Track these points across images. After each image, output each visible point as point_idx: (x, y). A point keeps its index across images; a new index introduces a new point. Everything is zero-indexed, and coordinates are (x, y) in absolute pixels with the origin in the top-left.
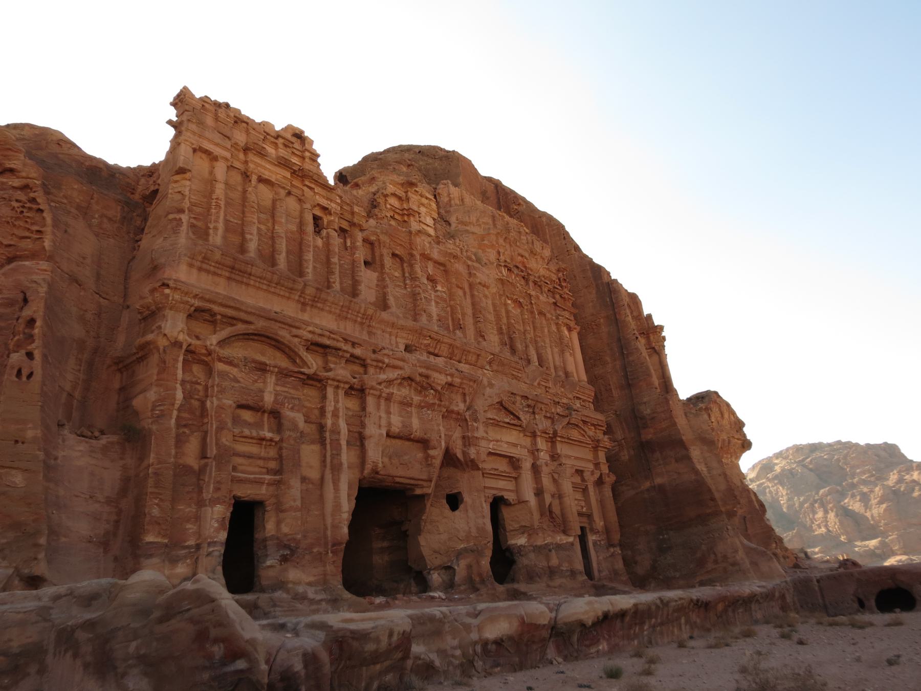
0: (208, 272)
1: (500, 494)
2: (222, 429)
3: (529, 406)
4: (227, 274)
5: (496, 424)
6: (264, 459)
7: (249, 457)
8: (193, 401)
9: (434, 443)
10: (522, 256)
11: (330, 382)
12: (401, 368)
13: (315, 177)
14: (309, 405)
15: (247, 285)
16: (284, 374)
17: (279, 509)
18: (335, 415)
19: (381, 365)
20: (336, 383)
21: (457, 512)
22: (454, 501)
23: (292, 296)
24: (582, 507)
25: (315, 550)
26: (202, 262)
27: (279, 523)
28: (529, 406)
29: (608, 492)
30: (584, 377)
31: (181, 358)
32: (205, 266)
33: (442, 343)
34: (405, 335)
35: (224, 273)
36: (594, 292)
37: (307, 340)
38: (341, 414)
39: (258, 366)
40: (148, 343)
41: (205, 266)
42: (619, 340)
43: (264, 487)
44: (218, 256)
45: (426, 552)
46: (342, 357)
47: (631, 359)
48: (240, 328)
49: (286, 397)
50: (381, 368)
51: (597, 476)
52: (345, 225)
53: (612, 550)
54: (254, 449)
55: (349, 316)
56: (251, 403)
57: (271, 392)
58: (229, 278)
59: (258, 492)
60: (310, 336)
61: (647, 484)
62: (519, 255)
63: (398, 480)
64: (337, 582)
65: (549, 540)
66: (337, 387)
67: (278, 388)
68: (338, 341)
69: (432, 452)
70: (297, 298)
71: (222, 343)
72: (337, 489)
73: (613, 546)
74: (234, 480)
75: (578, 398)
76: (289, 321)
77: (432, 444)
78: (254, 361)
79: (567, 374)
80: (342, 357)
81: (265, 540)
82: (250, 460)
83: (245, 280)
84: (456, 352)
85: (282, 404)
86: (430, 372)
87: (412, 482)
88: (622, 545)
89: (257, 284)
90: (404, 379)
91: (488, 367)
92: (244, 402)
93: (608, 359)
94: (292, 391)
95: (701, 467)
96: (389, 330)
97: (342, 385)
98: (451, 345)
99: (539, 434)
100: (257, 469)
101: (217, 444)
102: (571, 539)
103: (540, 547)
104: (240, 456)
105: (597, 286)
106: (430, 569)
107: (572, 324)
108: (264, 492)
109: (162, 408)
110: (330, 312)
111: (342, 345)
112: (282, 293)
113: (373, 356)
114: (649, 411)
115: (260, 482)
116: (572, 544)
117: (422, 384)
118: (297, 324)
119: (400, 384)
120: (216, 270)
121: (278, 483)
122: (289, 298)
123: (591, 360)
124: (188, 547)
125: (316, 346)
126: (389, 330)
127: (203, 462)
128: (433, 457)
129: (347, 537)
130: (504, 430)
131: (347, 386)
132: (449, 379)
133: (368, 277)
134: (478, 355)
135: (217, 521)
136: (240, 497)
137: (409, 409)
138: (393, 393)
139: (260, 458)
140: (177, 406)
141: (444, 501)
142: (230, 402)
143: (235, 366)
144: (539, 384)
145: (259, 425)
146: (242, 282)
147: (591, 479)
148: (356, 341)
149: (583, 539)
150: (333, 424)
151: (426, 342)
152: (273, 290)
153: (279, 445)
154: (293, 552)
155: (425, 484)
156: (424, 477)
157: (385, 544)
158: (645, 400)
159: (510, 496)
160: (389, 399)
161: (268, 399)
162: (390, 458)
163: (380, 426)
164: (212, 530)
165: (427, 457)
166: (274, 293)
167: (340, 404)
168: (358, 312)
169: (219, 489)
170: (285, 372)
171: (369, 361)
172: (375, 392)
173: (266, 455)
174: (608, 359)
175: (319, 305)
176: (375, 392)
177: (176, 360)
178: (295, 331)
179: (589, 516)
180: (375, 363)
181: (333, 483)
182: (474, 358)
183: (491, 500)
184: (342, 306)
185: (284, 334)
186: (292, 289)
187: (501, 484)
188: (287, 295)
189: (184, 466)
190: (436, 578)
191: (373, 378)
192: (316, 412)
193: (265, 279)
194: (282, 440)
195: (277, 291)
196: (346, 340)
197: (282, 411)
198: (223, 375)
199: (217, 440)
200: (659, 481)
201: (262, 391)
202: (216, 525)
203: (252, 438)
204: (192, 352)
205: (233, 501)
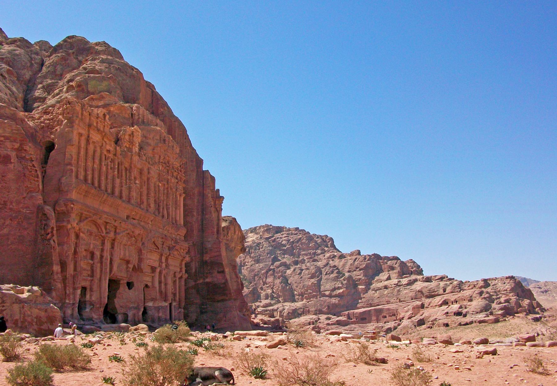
17: (91, 290)
18: (107, 252)
21: (131, 290)
22: (130, 285)
27: (91, 296)
29: (183, 283)
30: (182, 223)
36: (195, 174)
40: (63, 226)
42: (203, 205)
45: (117, 306)
47: (207, 216)
51: (180, 275)
61: (201, 281)
65: (160, 304)
69: (129, 265)
72: (105, 283)
73: (180, 308)
79: (176, 221)
81: (86, 301)
88: (185, 308)
93: (195, 214)
95: (228, 277)
105: (197, 171)
114: (210, 246)
121: (92, 280)
123: (187, 213)
133: (118, 181)
141: (126, 285)
147: (178, 276)
149: (171, 304)
158: (209, 240)
159: (150, 284)
165: (127, 267)
174: (195, 214)
190: (120, 317)
194: (94, 264)
200: (207, 280)
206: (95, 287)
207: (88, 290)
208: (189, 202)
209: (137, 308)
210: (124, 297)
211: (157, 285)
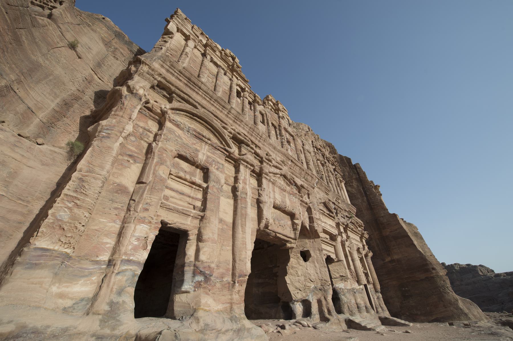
2: (162, 164)
4: (186, 82)
6: (193, 198)
7: (181, 193)
8: (142, 142)
9: (297, 216)
12: (281, 169)
14: (228, 173)
17: (200, 238)
19: (270, 163)
21: (308, 263)
23: (224, 111)
25: (225, 280)
26: (170, 67)
31: (139, 107)
34: (280, 156)
35: (183, 80)
39: (197, 135)
43: (190, 218)
45: (291, 288)
48: (188, 107)
49: (214, 161)
54: (187, 190)
55: (253, 135)
56: (188, 156)
57: (204, 154)
59: (183, 222)
61: (388, 259)
63: (278, 235)
64: (240, 309)
67: (209, 154)
70: (226, 113)
78: (195, 131)
82: (181, 196)
83: (196, 90)
85: (211, 164)
89: (204, 96)
92: (184, 154)
100: (186, 204)
101: (154, 173)
104: (174, 191)
105: (349, 166)
106: (295, 301)
107: (341, 179)
108: (189, 223)
109: (109, 132)
112: (217, 107)
114: (385, 221)
115: (186, 214)
120: (179, 76)
124: (97, 262)
127: (138, 185)
128: (297, 224)
129: (249, 271)
130: (327, 218)
135: (138, 239)
136: (167, 224)
137: (284, 193)
139: (189, 197)
140: (124, 135)
142: (173, 149)
143: (182, 129)
147: (364, 253)
150: (243, 187)
152: (212, 102)
153: (205, 192)
154: (207, 279)
155: (293, 241)
157: (260, 281)
159: (333, 256)
163: (270, 197)
164: (130, 247)
165: (294, 224)
168: (258, 134)
169: (147, 210)
170: (215, 145)
171: (264, 159)
172: (267, 177)
173: (195, 196)
175: (238, 122)
176: (267, 177)
177: (135, 108)
180: (267, 161)
181: (242, 226)
184: (250, 128)
186: (224, 107)
188: (221, 109)
189: (118, 185)
190: (298, 308)
191: (267, 168)
192: (233, 179)
193: (208, 94)
194: (207, 187)
195: (215, 105)
197: (210, 168)
198: (170, 131)
199: (155, 170)
202: (136, 243)
203: (185, 180)
205: (160, 226)
206: (211, 231)
207: (193, 237)
208: (350, 189)
209: (323, 290)
210: (300, 274)
211: (342, 257)
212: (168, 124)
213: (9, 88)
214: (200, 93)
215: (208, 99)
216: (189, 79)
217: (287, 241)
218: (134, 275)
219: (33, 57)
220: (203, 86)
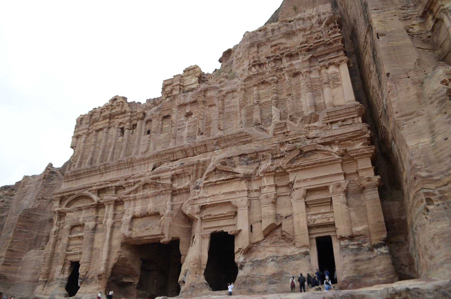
0: (70, 181)
1: (219, 230)
3: (252, 158)
4: (75, 178)
5: (215, 184)
9: (162, 213)
10: (275, 45)
11: (105, 204)
13: (116, 113)
15: (82, 178)
16: (88, 208)
19: (130, 184)
20: (107, 203)
23: (97, 173)
24: (329, 220)
28: (252, 158)
32: (69, 180)
33: (175, 152)
34: (153, 160)
37: (95, 190)
38: (109, 216)
41: (69, 180)
44: (70, 175)
46: (112, 189)
48: (71, 198)
49: (87, 217)
50: (131, 186)
52: (134, 122)
53: (376, 251)
55: (121, 167)
56: (75, 224)
58: (76, 179)
60: (94, 188)
62: (272, 47)
63: (145, 238)
66: (109, 204)
67: (86, 214)
68: (108, 184)
70: (99, 172)
71: (68, 206)
72: (102, 251)
74: (67, 255)
75: (331, 123)
76: (87, 186)
77: (161, 213)
78: (77, 208)
80: (112, 189)
83: (80, 177)
84: (188, 151)
85: (85, 221)
86: (159, 175)
87: (155, 237)
90: (144, 185)
91: (218, 148)
94: (91, 214)
96: (143, 163)
97: (110, 203)
98: (182, 150)
99: (261, 175)
100: (78, 249)
102: (303, 250)
103: (261, 261)
110: (113, 170)
111: (110, 185)
112: (93, 174)
113: (124, 182)
116: (306, 254)
117: (155, 183)
118: (90, 185)
119: (143, 189)
122: (96, 175)
125: (100, 192)
126: (143, 163)
130: (224, 185)
131: (113, 202)
132: (173, 172)
134: (205, 145)
137: (148, 200)
138: (135, 196)
144: (274, 135)
145: (82, 231)
146: (80, 179)
148: (115, 180)
151: (166, 157)
152: (89, 175)
155: (162, 237)
156: (159, 233)
160: (135, 199)
161: (81, 220)
162: (140, 228)
166: (91, 176)
167: (110, 212)
168: (125, 164)
171: (124, 186)
172: (126, 199)
176: (126, 199)
178: (90, 189)
179: (333, 225)
180: (127, 185)
182: (203, 149)
183: (209, 236)
184: (117, 165)
185: (86, 192)
186: (95, 170)
187: (222, 223)
188: (95, 174)
195: (91, 174)
196: (112, 182)
201: (79, 218)
204: (62, 213)
205: (70, 263)
212: (68, 214)
213: (37, 237)
214: (83, 176)
215: (87, 175)
216: (75, 175)
217: (158, 238)
218: (62, 284)
219: (39, 221)
220: (81, 172)
